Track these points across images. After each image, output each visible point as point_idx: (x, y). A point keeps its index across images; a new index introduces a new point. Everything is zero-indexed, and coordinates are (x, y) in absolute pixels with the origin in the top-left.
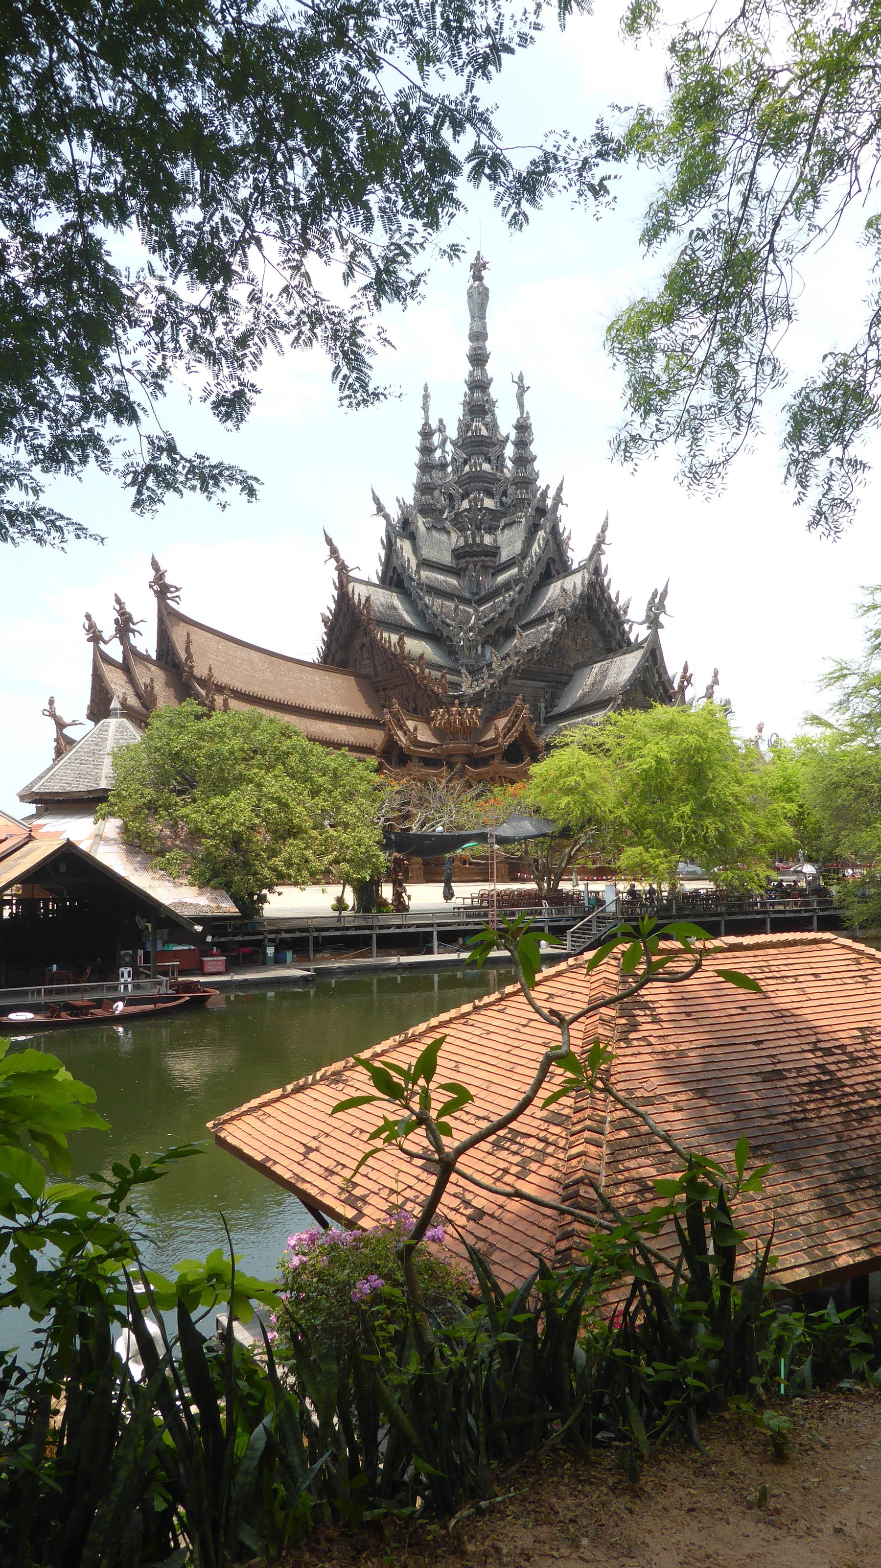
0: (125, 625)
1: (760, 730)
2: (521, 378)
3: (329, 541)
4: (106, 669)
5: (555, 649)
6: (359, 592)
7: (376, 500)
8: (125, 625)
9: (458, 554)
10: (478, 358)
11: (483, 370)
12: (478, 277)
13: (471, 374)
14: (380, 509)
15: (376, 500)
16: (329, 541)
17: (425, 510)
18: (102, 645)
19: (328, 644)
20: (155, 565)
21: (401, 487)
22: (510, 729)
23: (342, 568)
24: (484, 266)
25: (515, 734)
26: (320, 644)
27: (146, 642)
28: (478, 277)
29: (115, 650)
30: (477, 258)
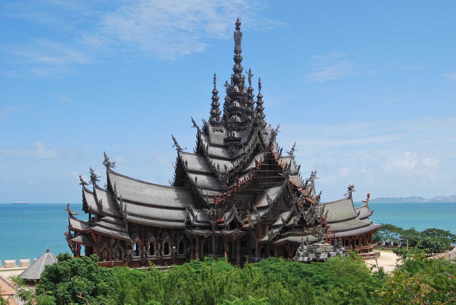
0: (94, 179)
1: (368, 196)
2: (250, 71)
3: (174, 139)
4: (86, 194)
5: (254, 183)
6: (185, 158)
7: (193, 122)
8: (94, 179)
9: (226, 140)
10: (238, 60)
11: (240, 65)
12: (238, 29)
13: (235, 66)
14: (195, 125)
15: (193, 122)
16: (174, 139)
17: (213, 123)
18: (85, 186)
19: (176, 176)
20: (105, 155)
21: (204, 115)
22: (230, 217)
23: (179, 150)
24: (240, 24)
25: (232, 219)
26: (174, 176)
27: (102, 183)
28: (238, 29)
29: (90, 187)
30: (238, 21)
